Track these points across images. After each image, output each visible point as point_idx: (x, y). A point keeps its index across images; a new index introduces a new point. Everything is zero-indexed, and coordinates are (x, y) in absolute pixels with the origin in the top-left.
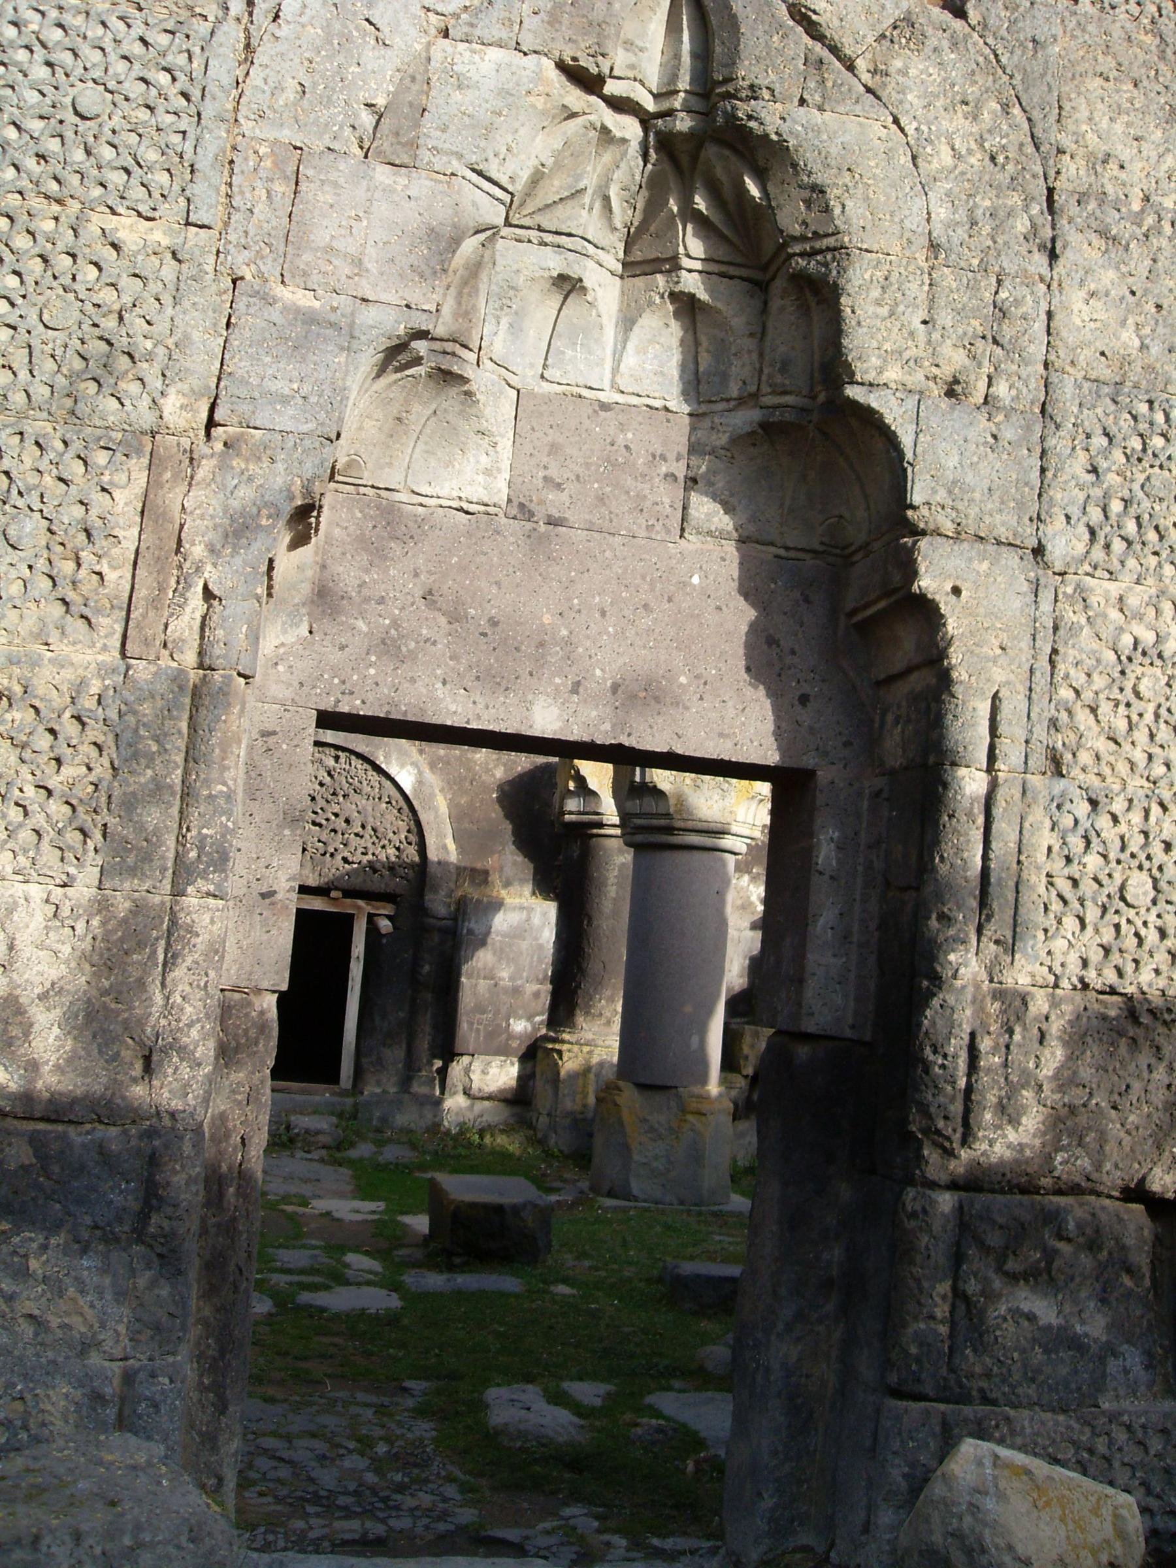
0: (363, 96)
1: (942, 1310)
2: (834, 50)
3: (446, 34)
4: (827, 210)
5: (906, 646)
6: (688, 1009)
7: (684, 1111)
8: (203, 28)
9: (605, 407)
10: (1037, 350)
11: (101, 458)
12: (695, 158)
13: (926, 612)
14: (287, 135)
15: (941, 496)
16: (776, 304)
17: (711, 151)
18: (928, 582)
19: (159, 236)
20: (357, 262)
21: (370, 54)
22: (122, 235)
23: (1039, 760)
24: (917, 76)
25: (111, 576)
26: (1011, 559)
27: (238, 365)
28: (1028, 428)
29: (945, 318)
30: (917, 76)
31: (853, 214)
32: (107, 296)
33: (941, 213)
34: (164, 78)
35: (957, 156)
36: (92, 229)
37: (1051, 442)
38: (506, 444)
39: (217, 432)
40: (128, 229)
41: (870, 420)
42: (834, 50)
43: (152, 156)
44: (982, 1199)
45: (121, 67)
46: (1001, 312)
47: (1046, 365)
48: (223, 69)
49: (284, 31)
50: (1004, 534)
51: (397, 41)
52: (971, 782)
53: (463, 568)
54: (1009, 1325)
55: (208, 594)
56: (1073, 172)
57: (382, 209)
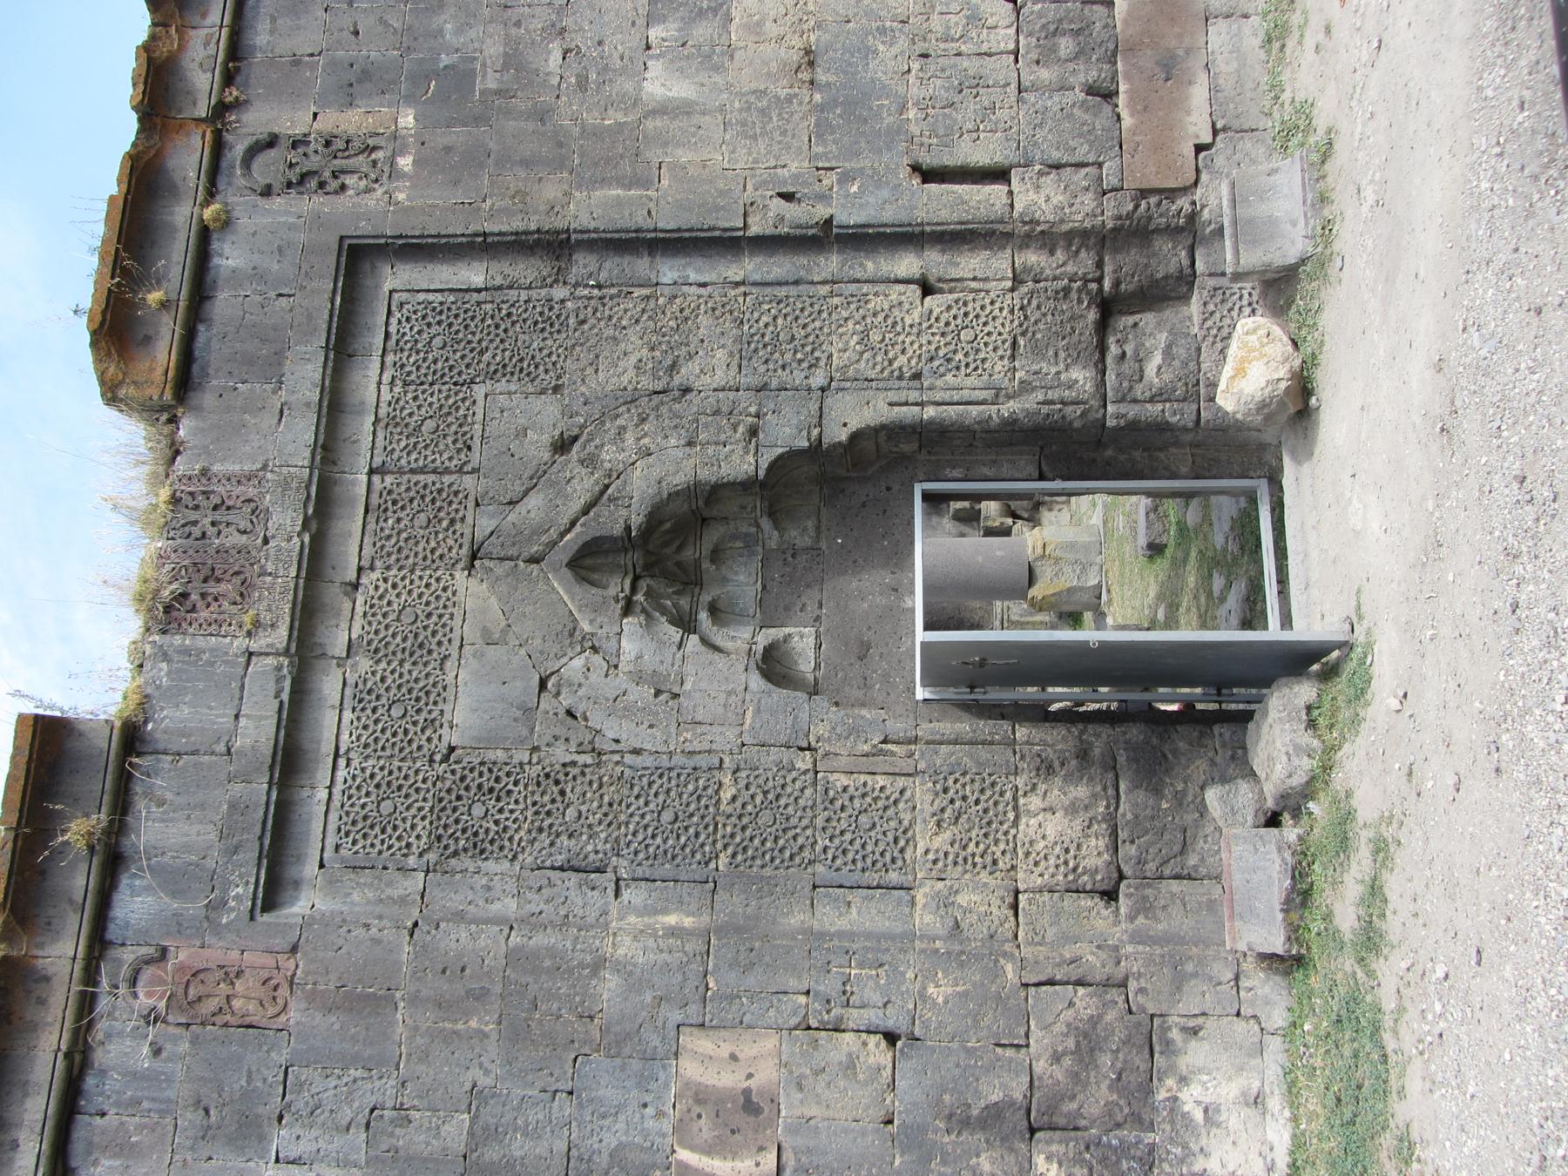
0: (651, 698)
1: (1160, 407)
2: (602, 493)
3: (616, 667)
4: (677, 493)
5: (869, 445)
6: (980, 559)
7: (1043, 556)
8: (628, 772)
9: (764, 587)
10: (732, 395)
11: (831, 793)
12: (652, 553)
13: (855, 437)
14: (673, 730)
15: (805, 433)
16: (714, 513)
17: (651, 547)
18: (843, 436)
19: (727, 779)
20: (729, 693)
21: (631, 698)
22: (729, 796)
23: (916, 384)
24: (610, 455)
25: (881, 783)
26: (828, 401)
27: (783, 739)
28: (768, 397)
29: (723, 437)
30: (610, 455)
31: (680, 479)
32: (758, 800)
33: (673, 442)
34: (655, 787)
35: (645, 435)
36: (729, 809)
37: (773, 386)
38: (787, 630)
39: (813, 744)
40: (726, 795)
41: (772, 466)
42: (602, 493)
43: (691, 787)
44: (1110, 394)
45: (652, 806)
46: (717, 413)
47: (738, 390)
48: (648, 761)
49: (624, 737)
50: (817, 406)
51: (624, 686)
52: (930, 412)
53: (846, 645)
54: (1164, 376)
55: (884, 742)
56: (646, 383)
57: (703, 685)
